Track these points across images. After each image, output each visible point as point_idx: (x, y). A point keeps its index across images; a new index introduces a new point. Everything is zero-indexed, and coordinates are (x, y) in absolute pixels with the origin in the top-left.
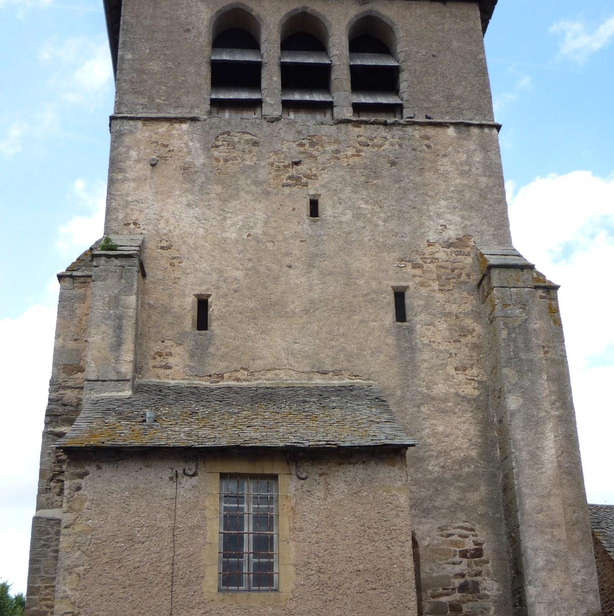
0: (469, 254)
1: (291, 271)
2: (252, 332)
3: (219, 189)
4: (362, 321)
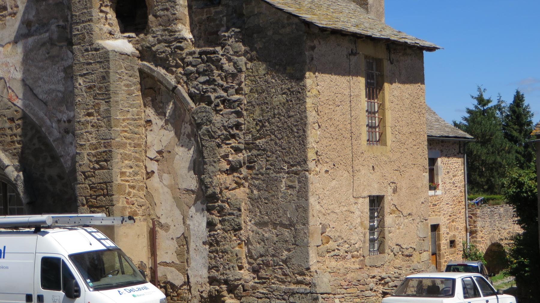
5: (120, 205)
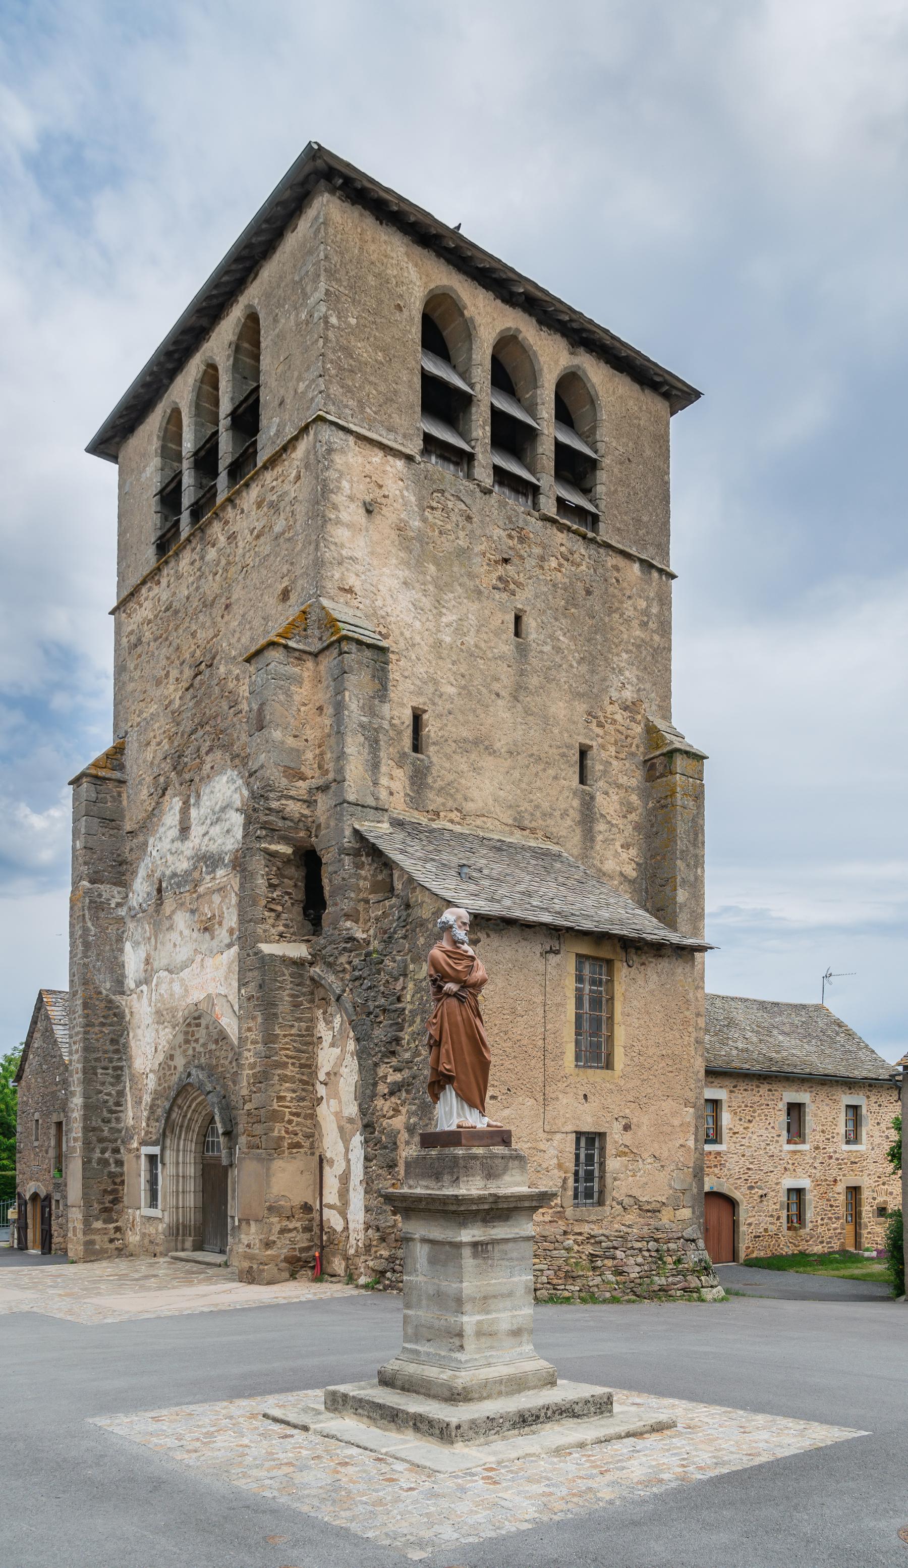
1: (499, 702)
2: (464, 767)
4: (556, 778)
5: (276, 1134)
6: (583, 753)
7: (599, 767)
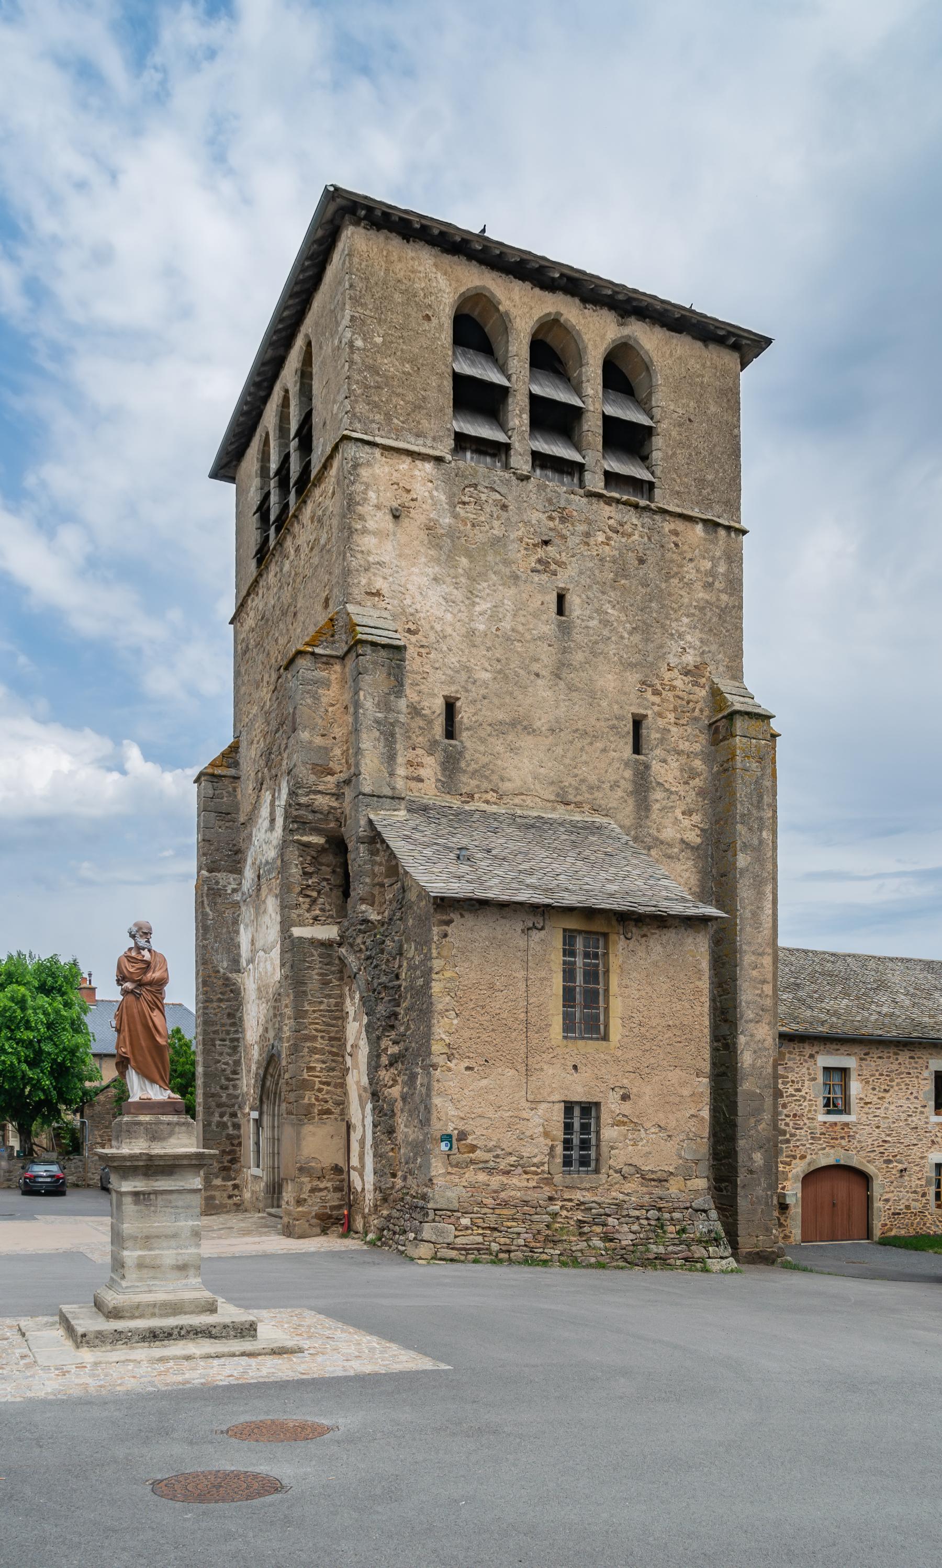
0: (703, 687)
1: (539, 682)
2: (500, 749)
3: (464, 561)
4: (604, 750)
5: (306, 1101)
6: (637, 723)
7: (655, 735)
